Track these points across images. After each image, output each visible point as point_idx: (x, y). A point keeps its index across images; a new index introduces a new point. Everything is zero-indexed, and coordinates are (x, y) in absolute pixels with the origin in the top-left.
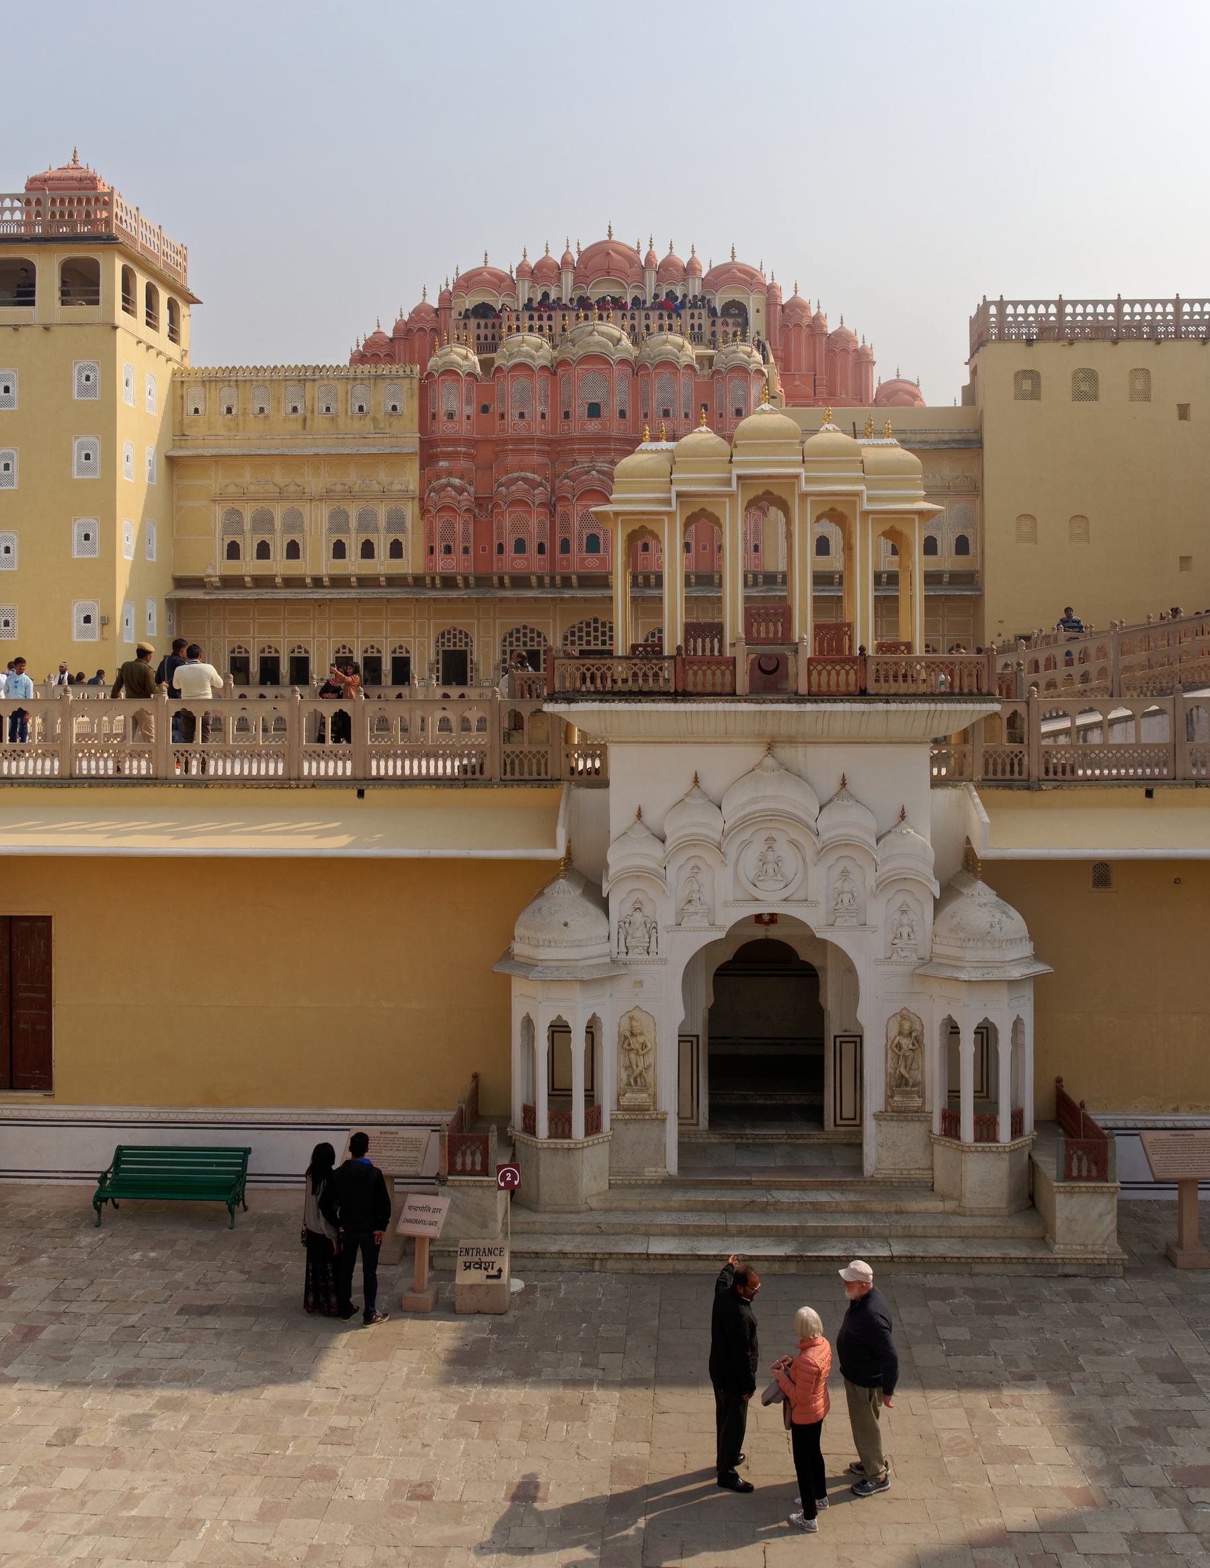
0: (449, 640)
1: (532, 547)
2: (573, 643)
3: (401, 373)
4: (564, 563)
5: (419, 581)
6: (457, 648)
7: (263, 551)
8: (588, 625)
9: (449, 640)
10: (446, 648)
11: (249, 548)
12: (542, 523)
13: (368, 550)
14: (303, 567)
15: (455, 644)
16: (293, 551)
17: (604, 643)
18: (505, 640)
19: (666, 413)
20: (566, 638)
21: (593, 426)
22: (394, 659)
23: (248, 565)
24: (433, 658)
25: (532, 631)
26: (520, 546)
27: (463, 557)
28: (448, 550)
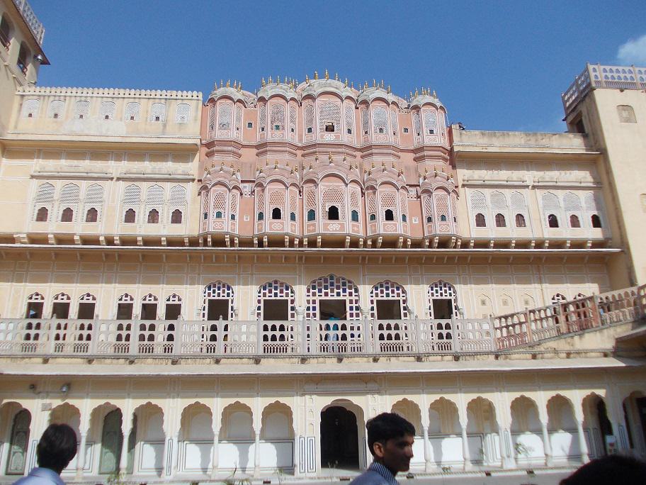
0: (214, 292)
1: (285, 214)
2: (314, 294)
3: (190, 97)
4: (311, 228)
5: (194, 242)
6: (221, 298)
7: (67, 215)
8: (326, 281)
9: (214, 292)
10: (211, 298)
11: (55, 213)
12: (293, 199)
13: (153, 216)
14: (99, 229)
15: (219, 295)
16: (92, 215)
17: (338, 294)
18: (260, 292)
19: (381, 130)
20: (308, 291)
21: (329, 137)
22: (167, 305)
23: (54, 226)
24: (201, 304)
25: (282, 284)
26: (277, 214)
27: (231, 221)
28: (219, 215)
